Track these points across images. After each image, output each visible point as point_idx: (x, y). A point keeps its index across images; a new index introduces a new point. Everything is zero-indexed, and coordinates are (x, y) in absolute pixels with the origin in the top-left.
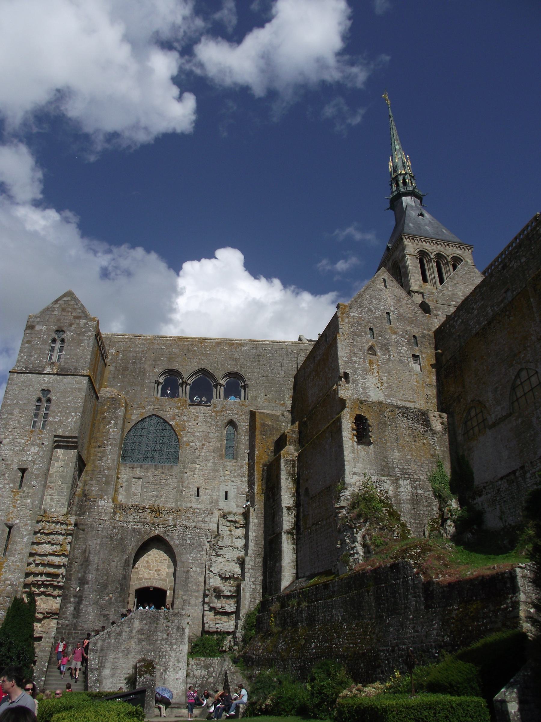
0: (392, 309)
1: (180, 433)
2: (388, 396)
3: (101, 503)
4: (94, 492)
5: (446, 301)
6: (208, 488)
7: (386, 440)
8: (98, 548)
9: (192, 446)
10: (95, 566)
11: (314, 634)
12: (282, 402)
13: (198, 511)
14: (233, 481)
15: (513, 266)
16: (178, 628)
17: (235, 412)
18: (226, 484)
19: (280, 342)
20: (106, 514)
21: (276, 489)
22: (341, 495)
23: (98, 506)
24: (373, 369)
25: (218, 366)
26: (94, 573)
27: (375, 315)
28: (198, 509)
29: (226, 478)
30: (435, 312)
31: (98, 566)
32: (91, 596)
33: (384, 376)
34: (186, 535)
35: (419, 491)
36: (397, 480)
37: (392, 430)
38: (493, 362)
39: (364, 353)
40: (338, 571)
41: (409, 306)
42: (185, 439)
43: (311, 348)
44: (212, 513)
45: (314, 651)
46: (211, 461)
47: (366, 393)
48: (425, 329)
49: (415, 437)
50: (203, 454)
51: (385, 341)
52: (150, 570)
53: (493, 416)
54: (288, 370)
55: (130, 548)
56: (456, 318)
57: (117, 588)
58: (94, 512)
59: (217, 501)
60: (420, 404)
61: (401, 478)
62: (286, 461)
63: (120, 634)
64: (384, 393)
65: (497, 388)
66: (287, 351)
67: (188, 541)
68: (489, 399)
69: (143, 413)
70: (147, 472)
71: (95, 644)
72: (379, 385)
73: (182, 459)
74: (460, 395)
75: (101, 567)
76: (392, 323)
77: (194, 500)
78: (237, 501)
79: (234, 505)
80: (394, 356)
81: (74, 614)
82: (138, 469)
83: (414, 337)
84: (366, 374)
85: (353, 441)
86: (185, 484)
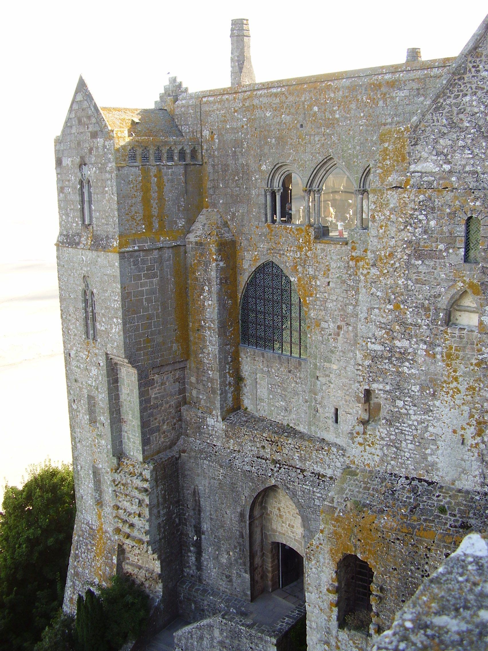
3: (210, 421)
4: (202, 402)
8: (207, 491)
9: (323, 329)
10: (208, 514)
20: (218, 438)
23: (208, 426)
24: (456, 379)
31: (211, 514)
32: (208, 551)
34: (314, 492)
39: (434, 322)
42: (312, 314)
47: (425, 457)
52: (283, 522)
55: (244, 498)
57: (235, 547)
58: (204, 433)
63: (201, 638)
67: (317, 502)
69: (256, 256)
70: (272, 367)
71: (180, 640)
72: (472, 430)
75: (214, 517)
77: (332, 428)
81: (196, 565)
86: (318, 397)
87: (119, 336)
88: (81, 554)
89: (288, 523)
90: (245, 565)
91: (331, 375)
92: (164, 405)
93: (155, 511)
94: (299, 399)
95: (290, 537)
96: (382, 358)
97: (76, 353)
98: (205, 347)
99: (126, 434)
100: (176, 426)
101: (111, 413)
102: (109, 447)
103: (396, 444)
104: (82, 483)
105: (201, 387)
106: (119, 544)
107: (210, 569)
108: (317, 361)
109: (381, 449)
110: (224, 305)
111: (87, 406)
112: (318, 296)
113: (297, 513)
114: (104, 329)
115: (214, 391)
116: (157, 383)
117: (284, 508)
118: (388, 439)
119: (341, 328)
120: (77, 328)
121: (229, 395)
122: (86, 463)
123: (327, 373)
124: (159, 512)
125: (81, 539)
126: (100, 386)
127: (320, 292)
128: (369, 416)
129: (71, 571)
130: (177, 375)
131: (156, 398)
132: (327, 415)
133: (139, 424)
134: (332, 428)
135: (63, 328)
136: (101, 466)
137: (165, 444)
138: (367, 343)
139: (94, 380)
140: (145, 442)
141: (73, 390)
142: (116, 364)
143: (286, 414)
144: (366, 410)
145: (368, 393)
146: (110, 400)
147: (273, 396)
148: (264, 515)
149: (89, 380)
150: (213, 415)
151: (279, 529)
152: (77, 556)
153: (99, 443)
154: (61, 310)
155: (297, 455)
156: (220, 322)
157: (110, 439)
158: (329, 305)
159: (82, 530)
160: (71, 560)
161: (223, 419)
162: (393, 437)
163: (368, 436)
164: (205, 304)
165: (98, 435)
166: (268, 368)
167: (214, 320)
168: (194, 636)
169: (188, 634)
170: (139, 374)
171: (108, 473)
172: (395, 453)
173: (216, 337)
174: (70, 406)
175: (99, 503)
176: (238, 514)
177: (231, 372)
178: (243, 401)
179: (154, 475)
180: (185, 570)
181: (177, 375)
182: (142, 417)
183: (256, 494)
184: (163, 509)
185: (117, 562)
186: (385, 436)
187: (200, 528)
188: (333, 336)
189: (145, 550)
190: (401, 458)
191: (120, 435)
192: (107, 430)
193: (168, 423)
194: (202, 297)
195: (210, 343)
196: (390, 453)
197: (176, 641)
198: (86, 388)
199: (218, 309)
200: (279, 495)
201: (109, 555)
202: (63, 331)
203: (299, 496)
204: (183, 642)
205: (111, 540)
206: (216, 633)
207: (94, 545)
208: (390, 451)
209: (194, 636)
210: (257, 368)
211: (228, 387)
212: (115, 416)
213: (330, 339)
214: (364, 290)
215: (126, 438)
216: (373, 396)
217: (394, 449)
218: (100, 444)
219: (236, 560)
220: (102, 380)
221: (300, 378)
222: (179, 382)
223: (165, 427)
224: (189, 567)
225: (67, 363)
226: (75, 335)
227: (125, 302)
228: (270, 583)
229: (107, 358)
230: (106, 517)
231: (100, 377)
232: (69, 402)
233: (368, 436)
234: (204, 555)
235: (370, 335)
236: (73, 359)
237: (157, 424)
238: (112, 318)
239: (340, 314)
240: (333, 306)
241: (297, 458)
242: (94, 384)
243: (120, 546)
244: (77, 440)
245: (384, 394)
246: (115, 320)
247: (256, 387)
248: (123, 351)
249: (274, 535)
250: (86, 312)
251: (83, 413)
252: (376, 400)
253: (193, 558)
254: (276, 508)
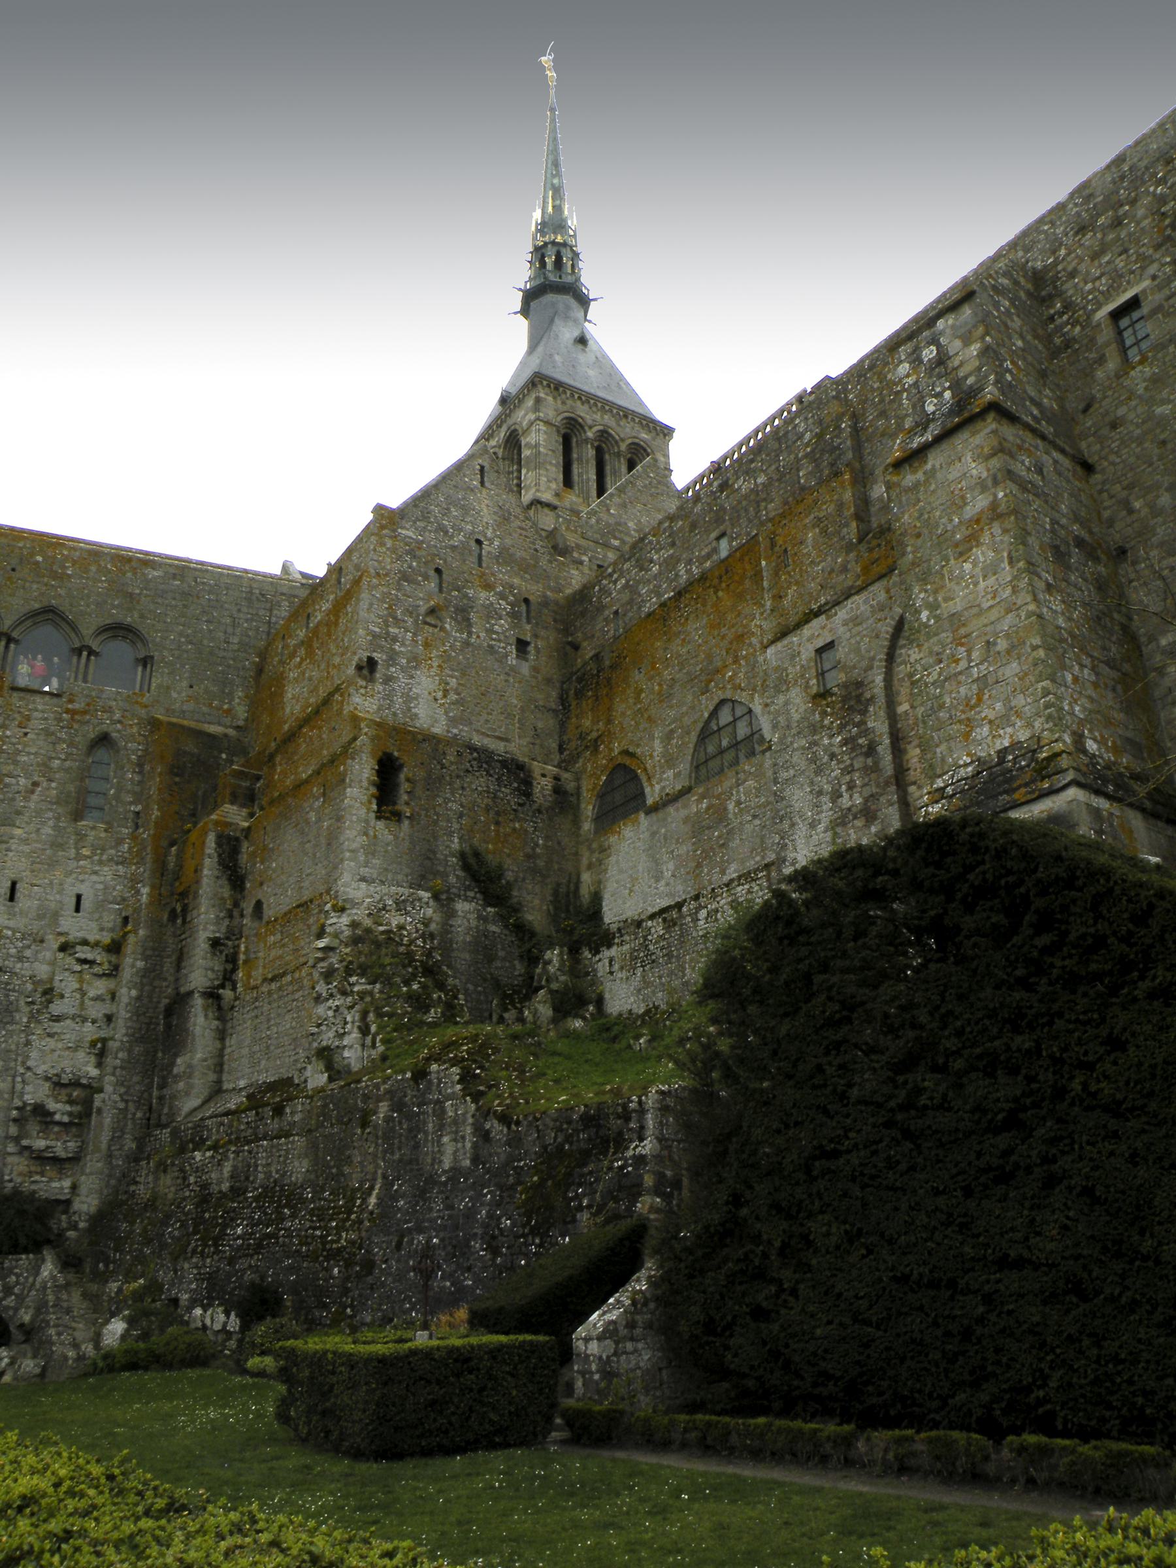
0: (489, 534)
2: (453, 721)
5: (603, 535)
6: (38, 882)
7: (437, 814)
9: (7, 785)
11: (243, 1208)
12: (226, 707)
13: (10, 933)
14: (95, 873)
15: (740, 488)
17: (117, 716)
18: (81, 877)
19: (238, 570)
21: (191, 897)
22: (329, 922)
24: (430, 659)
25: (88, 606)
27: (452, 542)
28: (8, 928)
29: (81, 863)
30: (575, 555)
33: (452, 677)
35: (493, 928)
36: (450, 900)
37: (453, 794)
38: (673, 679)
40: (306, 1081)
41: (524, 533)
43: (304, 593)
44: (42, 941)
45: (239, 1242)
46: (51, 823)
47: (409, 709)
48: (550, 588)
49: (498, 813)
50: (32, 805)
51: (465, 601)
53: (657, 787)
54: (249, 636)
56: (615, 576)
59: (56, 915)
60: (517, 748)
61: (459, 896)
62: (221, 840)
64: (446, 713)
65: (672, 732)
66: (251, 592)
68: (655, 754)
72: (440, 694)
74: (599, 737)
76: (484, 565)
78: (101, 917)
79: (94, 925)
80: (478, 637)
83: (526, 601)
84: (415, 668)
85: (368, 809)
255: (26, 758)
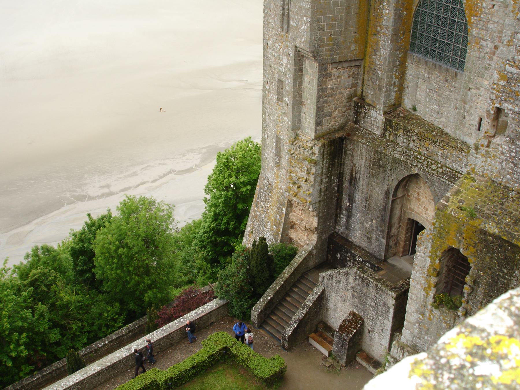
1: (470, 19)
3: (374, 113)
9: (482, 47)
16: (384, 304)
20: (378, 128)
23: (371, 117)
26: (360, 193)
31: (363, 188)
32: (357, 216)
34: (449, 185)
42: (474, 32)
52: (420, 205)
57: (378, 217)
58: (368, 122)
63: (339, 281)
70: (432, 74)
73: (469, 66)
77: (474, 134)
81: (345, 225)
82: (424, 66)
87: (307, 33)
88: (261, 202)
89: (423, 205)
90: (383, 233)
91: (482, 89)
92: (338, 95)
93: (319, 179)
94: (450, 105)
95: (423, 217)
96: (517, 80)
97: (273, 44)
98: (378, 50)
99: (304, 115)
100: (346, 113)
101: (294, 96)
102: (290, 123)
103: (515, 161)
104: (267, 148)
105: (370, 83)
106: (288, 200)
107: (356, 230)
108: (472, 75)
109: (500, 163)
110: (399, 15)
111: (276, 88)
112: (482, 16)
113: (432, 200)
114: (296, 25)
115: (380, 89)
116: (334, 76)
117: (422, 193)
118: (508, 155)
119: (498, 48)
120: (275, 22)
121: (393, 94)
122: (272, 133)
123: (478, 86)
124: (322, 180)
125: (262, 191)
126: (288, 73)
127: (485, 13)
128: (496, 132)
129: (252, 213)
130: (352, 71)
131: (332, 89)
132: (472, 122)
133: (315, 108)
134: (474, 134)
135: (264, 21)
136: (282, 137)
137: (334, 127)
138: (505, 65)
139: (284, 67)
140: (319, 123)
141: (268, 74)
142: (303, 56)
143: (438, 117)
144: (494, 125)
145: (499, 111)
146: (294, 86)
147: (430, 99)
148: (406, 197)
149: (280, 67)
150: (377, 109)
151: (416, 209)
152: (257, 203)
153: (282, 119)
154: (264, 6)
155: (441, 152)
156: (394, 30)
157: (291, 117)
158: (491, 26)
159: (263, 184)
160: (253, 205)
161: (385, 114)
162: (513, 154)
163: (491, 149)
164: (384, 13)
165: (282, 113)
166: (429, 75)
167: (389, 28)
168: (334, 279)
169: (330, 276)
170: (319, 66)
171: (287, 143)
172: (512, 169)
173: (388, 43)
174: (264, 87)
175: (278, 165)
176: (384, 192)
177: (397, 74)
178: (404, 100)
179: (322, 151)
180: (337, 227)
181: (352, 71)
182: (318, 102)
183: (401, 178)
184: (325, 178)
185: (286, 212)
186: (506, 152)
187: (353, 197)
188: (489, 55)
189: (307, 208)
190: (517, 174)
191: (300, 115)
192: (289, 109)
193: (339, 110)
194: (381, 6)
195: (383, 47)
196: (508, 168)
197: (320, 279)
198: (277, 73)
199: (394, 18)
200: (420, 182)
201: (281, 206)
202: (264, 24)
203: (436, 186)
204: (326, 281)
205: (283, 195)
206: (351, 280)
207: (271, 197)
208: (508, 166)
209: (334, 279)
210: (420, 74)
211: (392, 86)
212: (297, 99)
213: (486, 57)
214: (511, 14)
215: (304, 118)
216: (502, 115)
217: (512, 165)
218: (283, 120)
219: (377, 227)
220: (290, 67)
221: (454, 87)
222: (353, 77)
223: (336, 113)
224: (340, 226)
225: (265, 51)
226: (273, 28)
227: (315, 3)
228: (401, 249)
229: (296, 50)
230: (281, 177)
231: (289, 66)
232: (263, 84)
233: (491, 149)
234: (353, 218)
235: (510, 58)
236: (270, 48)
237: (330, 110)
238: (302, 17)
239: (498, 35)
240: (494, 27)
241: (440, 155)
242: (283, 71)
243: (289, 201)
244: (267, 114)
245: (512, 114)
246: (305, 18)
247: (416, 89)
248: (308, 46)
249: (411, 213)
250: (283, 9)
251: (273, 93)
252: (505, 118)
253: (344, 219)
254: (416, 192)
255: (492, 26)
